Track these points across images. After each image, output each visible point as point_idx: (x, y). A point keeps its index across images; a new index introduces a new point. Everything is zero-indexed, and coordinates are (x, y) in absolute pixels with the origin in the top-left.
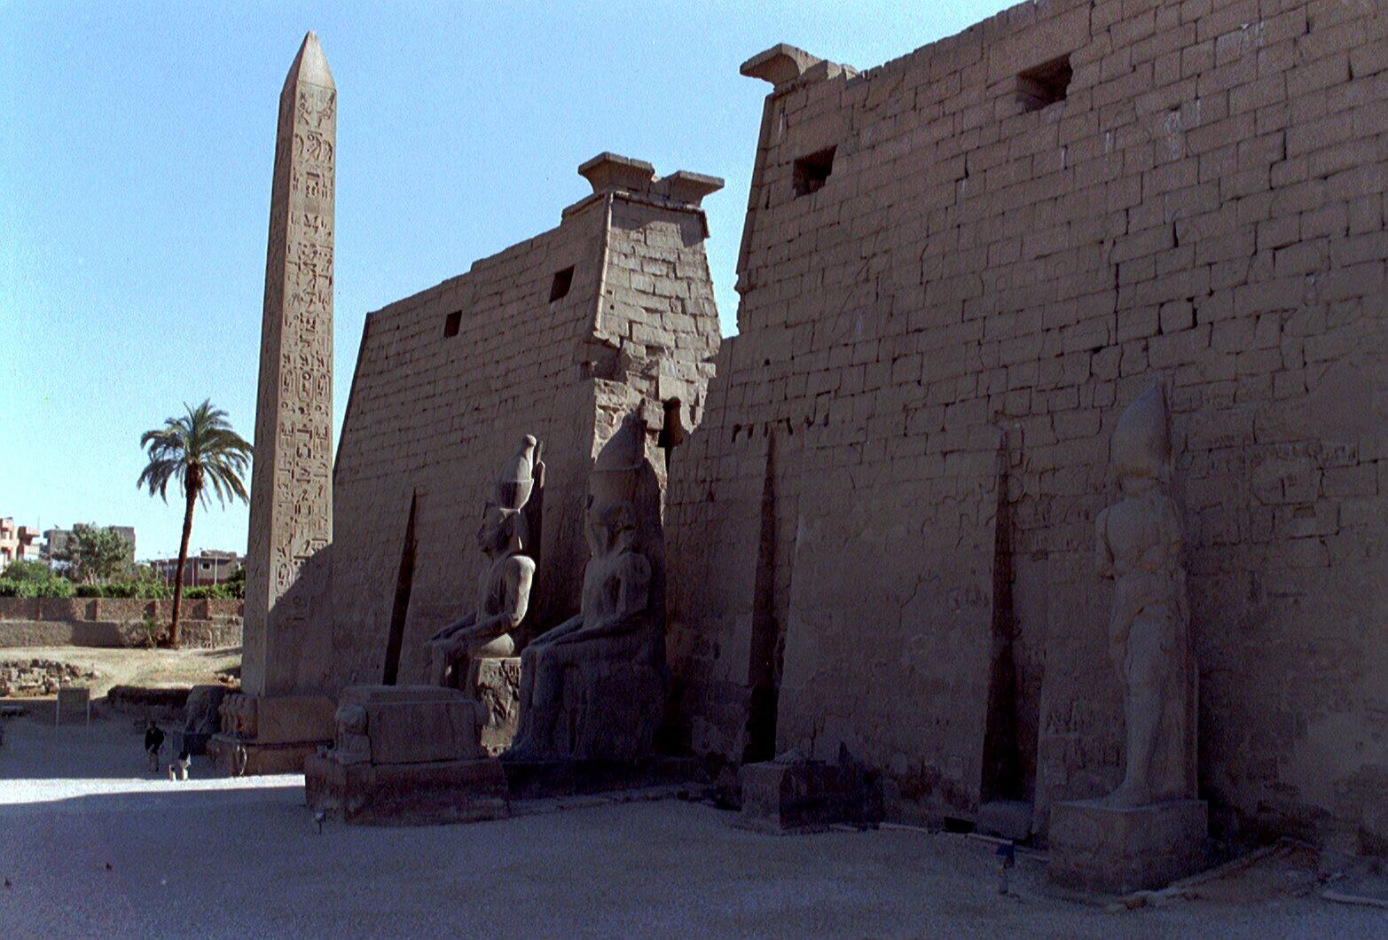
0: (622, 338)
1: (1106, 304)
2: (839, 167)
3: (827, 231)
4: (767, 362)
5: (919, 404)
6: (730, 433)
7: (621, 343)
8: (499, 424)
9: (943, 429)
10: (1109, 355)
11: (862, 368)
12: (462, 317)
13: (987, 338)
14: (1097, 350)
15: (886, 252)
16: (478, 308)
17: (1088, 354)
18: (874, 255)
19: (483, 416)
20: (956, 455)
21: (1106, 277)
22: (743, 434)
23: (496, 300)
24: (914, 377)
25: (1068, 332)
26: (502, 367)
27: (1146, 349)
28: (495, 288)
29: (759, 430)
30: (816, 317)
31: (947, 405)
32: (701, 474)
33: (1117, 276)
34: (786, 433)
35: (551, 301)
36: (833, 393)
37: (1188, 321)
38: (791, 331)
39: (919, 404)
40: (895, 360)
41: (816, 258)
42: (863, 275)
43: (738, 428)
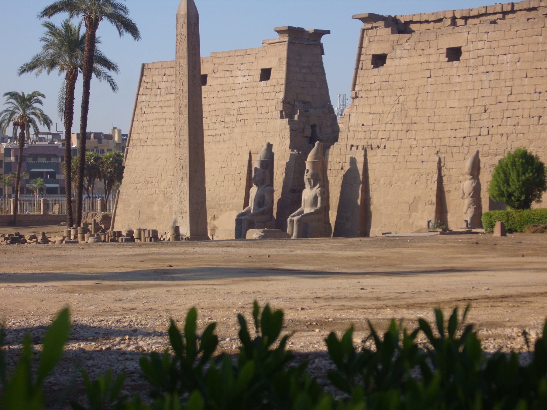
0: (294, 101)
1: (467, 125)
2: (388, 61)
3: (384, 83)
4: (363, 125)
5: (414, 146)
6: (350, 147)
7: (294, 102)
8: (237, 130)
9: (422, 154)
10: (468, 139)
11: (397, 132)
12: (208, 78)
13: (435, 129)
14: (464, 137)
15: (405, 95)
16: (217, 75)
17: (462, 138)
18: (401, 96)
19: (227, 125)
20: (426, 162)
21: (467, 118)
22: (354, 148)
23: (228, 74)
24: (413, 137)
25: (458, 131)
26: (236, 105)
27: (477, 139)
28: (227, 68)
29: (360, 148)
30: (381, 112)
31: (424, 147)
32: (339, 160)
33: (470, 118)
34: (370, 149)
35: (261, 81)
36: (387, 139)
37: (487, 133)
38: (371, 116)
39: (414, 146)
40: (407, 131)
41: (380, 92)
42: (397, 102)
43: (352, 146)
